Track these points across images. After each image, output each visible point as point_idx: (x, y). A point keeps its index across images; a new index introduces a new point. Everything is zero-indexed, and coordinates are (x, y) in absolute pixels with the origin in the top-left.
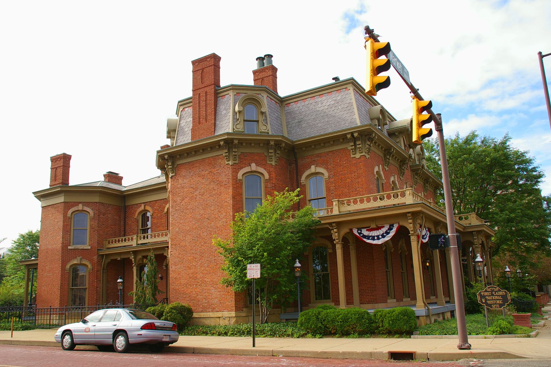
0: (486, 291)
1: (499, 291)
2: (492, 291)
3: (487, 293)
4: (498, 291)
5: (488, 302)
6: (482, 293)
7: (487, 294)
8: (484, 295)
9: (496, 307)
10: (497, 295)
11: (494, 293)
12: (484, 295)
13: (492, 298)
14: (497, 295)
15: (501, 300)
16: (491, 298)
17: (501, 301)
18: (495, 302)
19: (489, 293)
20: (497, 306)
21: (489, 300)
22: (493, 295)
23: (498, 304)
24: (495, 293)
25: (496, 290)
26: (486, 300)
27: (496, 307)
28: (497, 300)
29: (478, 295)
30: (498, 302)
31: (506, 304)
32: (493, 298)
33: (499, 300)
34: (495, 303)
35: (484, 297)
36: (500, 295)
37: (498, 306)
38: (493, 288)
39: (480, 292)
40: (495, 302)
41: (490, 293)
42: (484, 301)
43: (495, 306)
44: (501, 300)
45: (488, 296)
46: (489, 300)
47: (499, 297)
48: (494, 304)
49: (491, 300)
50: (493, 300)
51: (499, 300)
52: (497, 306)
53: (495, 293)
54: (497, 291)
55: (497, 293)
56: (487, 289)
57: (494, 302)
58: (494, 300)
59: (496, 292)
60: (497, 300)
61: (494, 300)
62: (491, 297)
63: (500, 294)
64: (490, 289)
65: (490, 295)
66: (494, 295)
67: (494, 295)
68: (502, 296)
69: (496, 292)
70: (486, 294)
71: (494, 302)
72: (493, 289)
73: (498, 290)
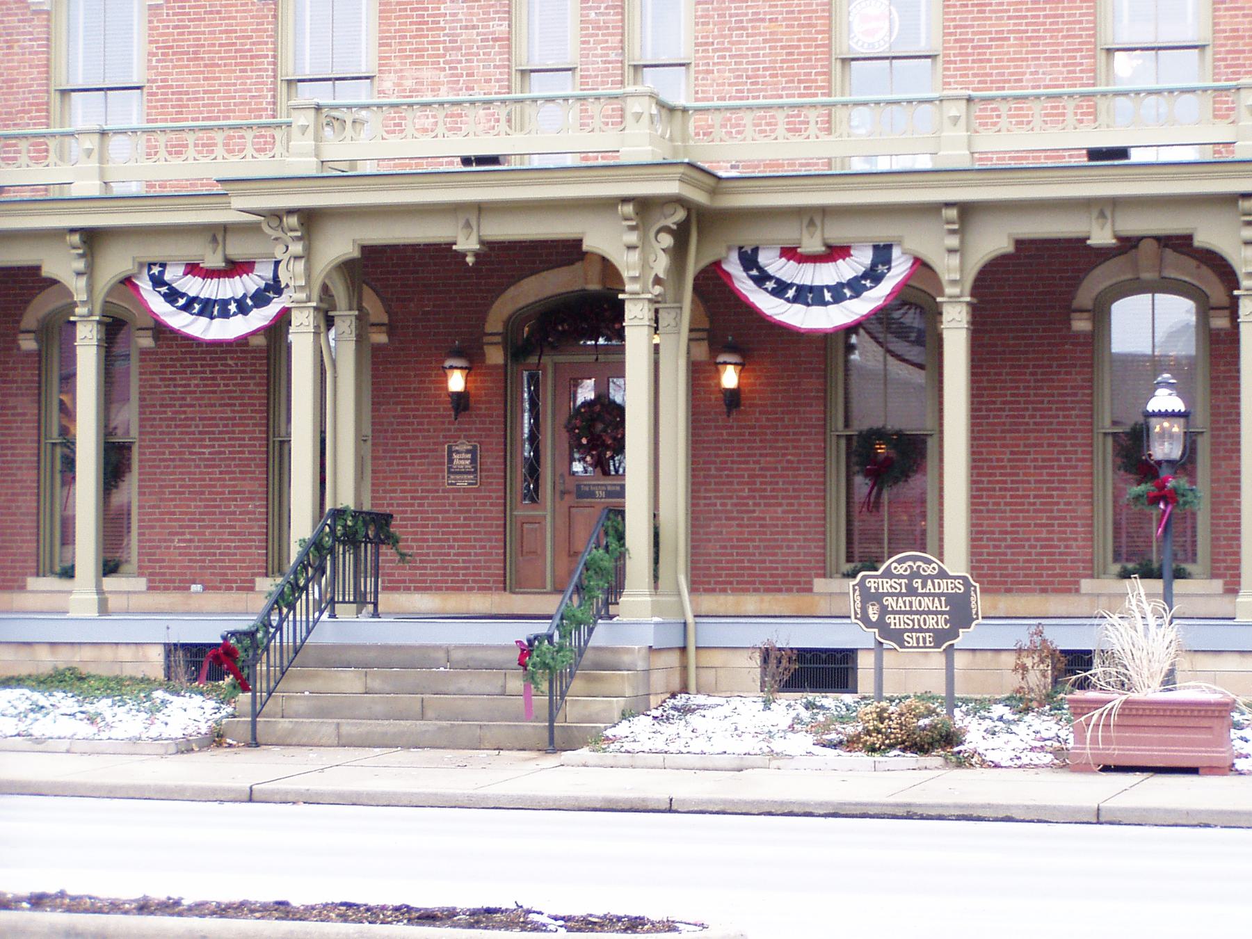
0: (888, 574)
2: (915, 575)
3: (892, 582)
4: (937, 577)
5: (891, 620)
6: (871, 584)
7: (891, 586)
8: (877, 589)
9: (921, 644)
12: (877, 589)
13: (911, 603)
15: (942, 613)
16: (904, 602)
17: (941, 619)
18: (919, 620)
19: (900, 585)
20: (924, 639)
21: (894, 612)
22: (912, 591)
23: (928, 630)
24: (924, 585)
25: (929, 572)
26: (884, 611)
27: (921, 644)
28: (929, 612)
29: (854, 590)
30: (931, 622)
31: (961, 630)
32: (911, 606)
33: (936, 613)
34: (916, 627)
35: (878, 597)
36: (943, 594)
37: (928, 639)
38: (919, 563)
40: (919, 620)
41: (904, 581)
42: (874, 618)
43: (918, 639)
44: (942, 613)
45: (891, 595)
46: (894, 612)
47: (936, 599)
48: (913, 630)
50: (911, 612)
51: (936, 613)
52: (924, 639)
53: (924, 585)
54: (932, 577)
55: (933, 584)
56: (895, 565)
57: (913, 621)
58: (917, 613)
59: (929, 582)
60: (929, 612)
61: (917, 613)
62: (907, 599)
63: (944, 589)
64: (905, 565)
65: (904, 591)
66: (920, 591)
67: (920, 591)
68: (951, 599)
69: (929, 582)
70: (887, 585)
71: (913, 621)
72: (919, 567)
73: (936, 572)
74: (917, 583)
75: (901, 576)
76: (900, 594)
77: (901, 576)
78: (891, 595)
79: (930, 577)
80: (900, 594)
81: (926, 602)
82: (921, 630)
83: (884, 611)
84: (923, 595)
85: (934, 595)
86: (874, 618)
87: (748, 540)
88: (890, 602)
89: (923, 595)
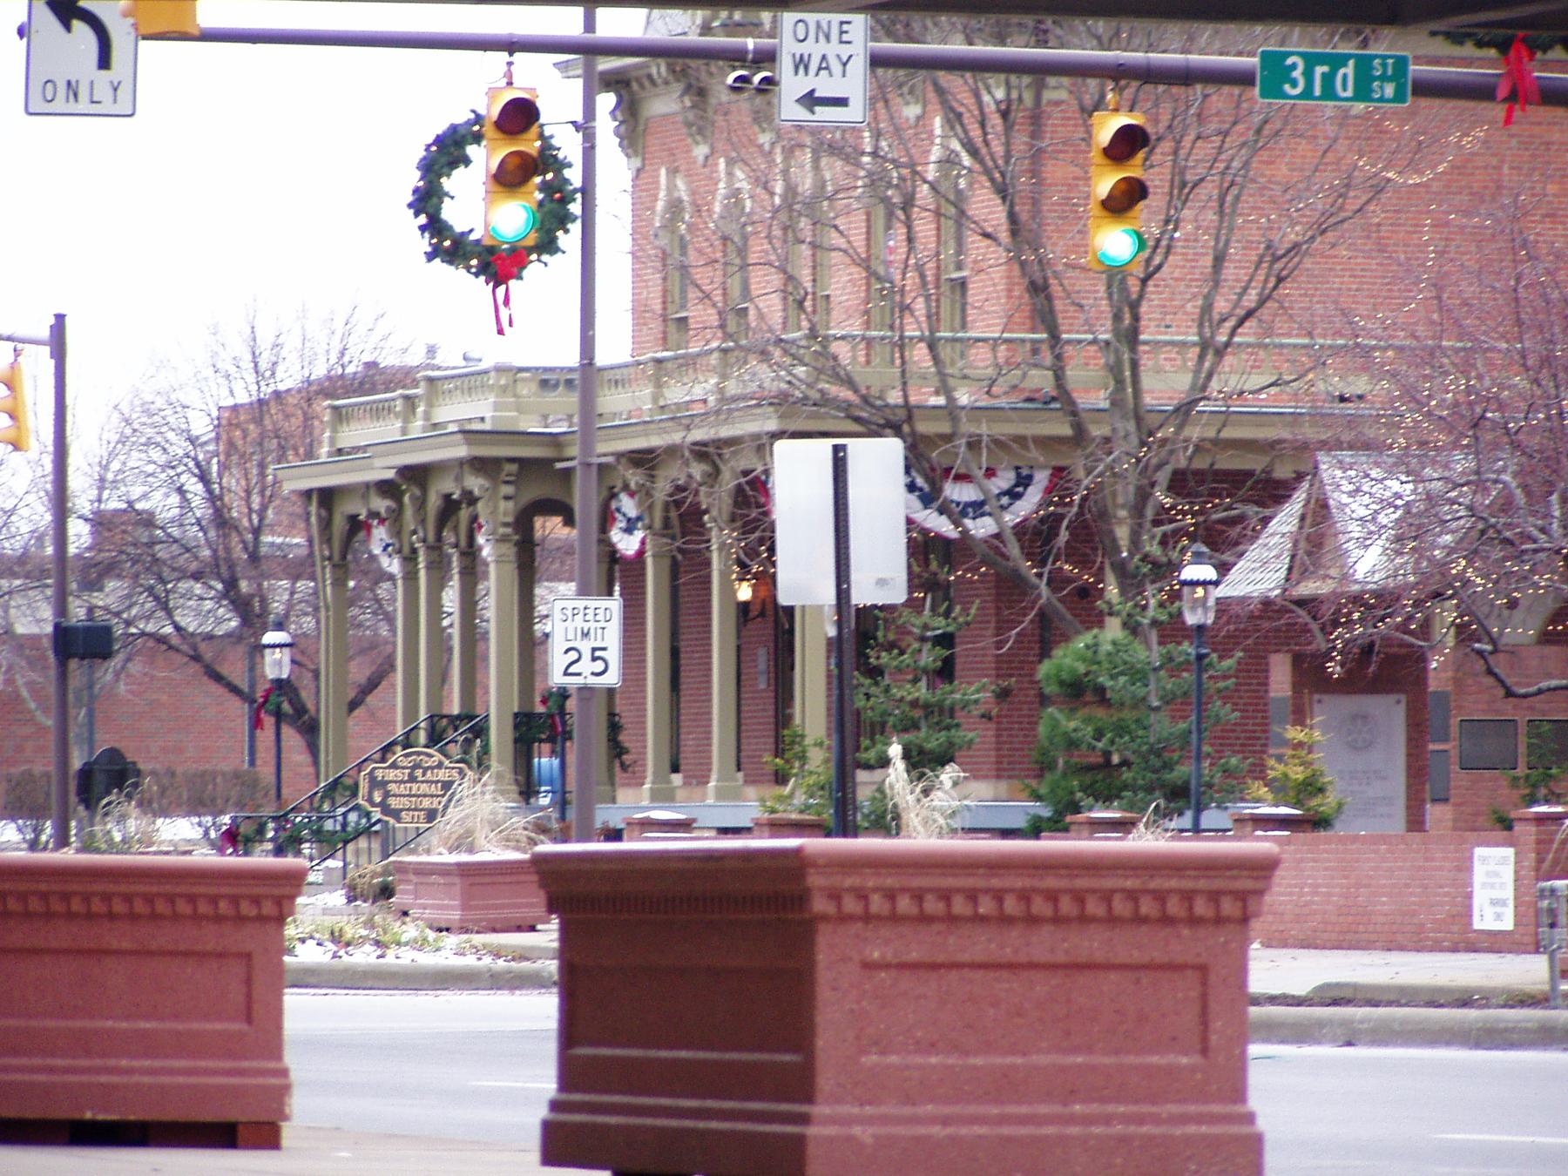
0: (394, 766)
1: (440, 765)
2: (416, 766)
5: (394, 803)
6: (379, 774)
10: (427, 782)
11: (419, 773)
13: (411, 789)
14: (427, 782)
22: (412, 779)
24: (424, 775)
28: (425, 796)
33: (432, 796)
35: (384, 784)
36: (438, 782)
39: (375, 768)
41: (407, 771)
42: (378, 799)
45: (396, 782)
48: (408, 810)
49: (404, 796)
51: (432, 796)
53: (424, 775)
58: (414, 796)
60: (425, 796)
61: (414, 796)
66: (420, 779)
67: (420, 779)
70: (391, 774)
74: (419, 773)
75: (404, 768)
76: (402, 782)
77: (404, 768)
78: (396, 782)
79: (429, 768)
80: (402, 782)
81: (424, 788)
82: (415, 810)
83: (387, 795)
84: (422, 782)
85: (432, 782)
86: (378, 799)
87: (1250, 704)
88: (392, 787)
89: (422, 782)
